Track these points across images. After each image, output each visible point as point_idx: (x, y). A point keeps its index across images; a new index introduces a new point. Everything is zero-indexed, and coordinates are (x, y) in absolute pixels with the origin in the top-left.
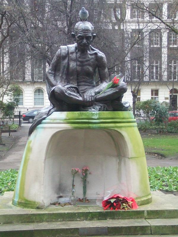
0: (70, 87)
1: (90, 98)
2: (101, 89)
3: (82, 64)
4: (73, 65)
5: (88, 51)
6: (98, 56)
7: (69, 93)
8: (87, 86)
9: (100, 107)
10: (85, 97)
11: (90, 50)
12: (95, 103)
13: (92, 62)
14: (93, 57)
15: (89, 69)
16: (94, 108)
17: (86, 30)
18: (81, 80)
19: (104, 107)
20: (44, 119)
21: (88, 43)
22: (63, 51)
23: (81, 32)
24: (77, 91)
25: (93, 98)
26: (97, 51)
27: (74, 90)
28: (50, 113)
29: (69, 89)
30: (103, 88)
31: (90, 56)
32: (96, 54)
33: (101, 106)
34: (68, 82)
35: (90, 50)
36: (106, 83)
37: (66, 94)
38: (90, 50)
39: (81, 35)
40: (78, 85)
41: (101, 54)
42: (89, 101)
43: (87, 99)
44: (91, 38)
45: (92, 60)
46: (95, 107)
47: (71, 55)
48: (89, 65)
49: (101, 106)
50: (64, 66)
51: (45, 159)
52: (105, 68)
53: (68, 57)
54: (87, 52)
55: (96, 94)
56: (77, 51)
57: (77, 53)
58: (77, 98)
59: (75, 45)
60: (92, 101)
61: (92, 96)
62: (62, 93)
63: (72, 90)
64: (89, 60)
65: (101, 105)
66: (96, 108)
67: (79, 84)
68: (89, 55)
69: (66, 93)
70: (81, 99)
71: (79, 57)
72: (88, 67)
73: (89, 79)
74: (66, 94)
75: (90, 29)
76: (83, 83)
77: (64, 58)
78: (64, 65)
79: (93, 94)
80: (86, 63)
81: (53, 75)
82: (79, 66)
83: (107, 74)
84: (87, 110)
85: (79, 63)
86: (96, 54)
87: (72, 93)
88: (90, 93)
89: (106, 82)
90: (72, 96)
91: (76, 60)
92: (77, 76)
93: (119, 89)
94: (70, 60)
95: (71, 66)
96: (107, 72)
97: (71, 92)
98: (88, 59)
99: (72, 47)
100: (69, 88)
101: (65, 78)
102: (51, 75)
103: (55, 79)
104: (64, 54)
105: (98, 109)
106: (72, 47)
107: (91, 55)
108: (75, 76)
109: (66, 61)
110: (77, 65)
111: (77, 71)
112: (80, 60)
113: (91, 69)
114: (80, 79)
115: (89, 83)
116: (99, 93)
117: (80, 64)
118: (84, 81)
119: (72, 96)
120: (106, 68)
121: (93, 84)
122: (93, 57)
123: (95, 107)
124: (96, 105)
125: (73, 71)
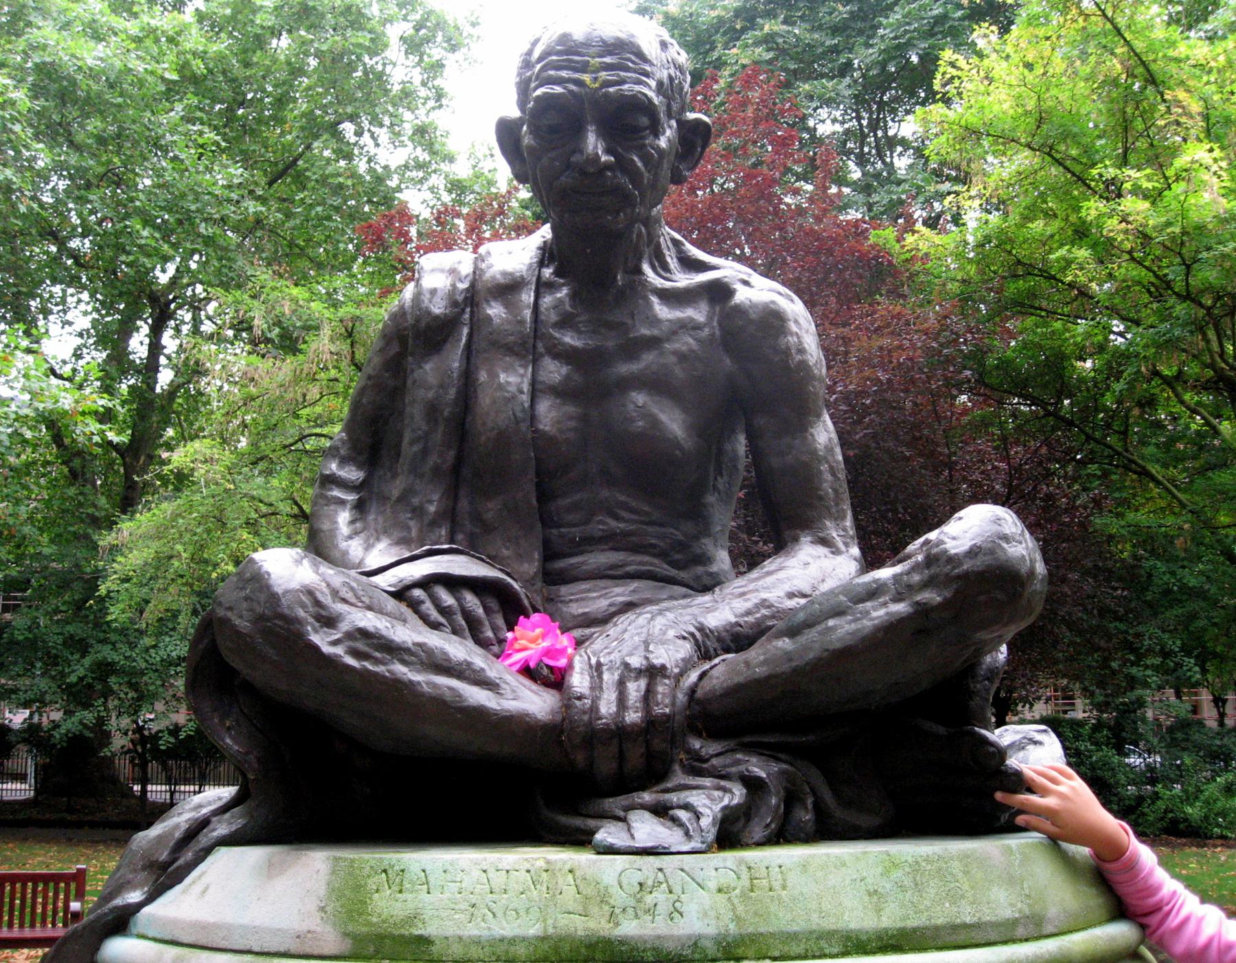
0: (427, 583)
1: (635, 689)
2: (764, 603)
5: (646, 268)
6: (740, 310)
7: (363, 633)
8: (635, 584)
9: (737, 794)
10: (579, 681)
11: (673, 263)
12: (689, 751)
13: (682, 357)
15: (655, 423)
16: (661, 811)
18: (576, 532)
19: (791, 799)
21: (622, 165)
23: (558, 68)
25: (662, 688)
27: (468, 616)
28: (189, 855)
29: (415, 606)
30: (791, 595)
31: (662, 311)
32: (719, 292)
33: (753, 785)
35: (666, 267)
36: (822, 550)
37: (316, 649)
38: (673, 263)
39: (558, 89)
42: (620, 733)
43: (594, 708)
44: (656, 131)
45: (687, 342)
46: (674, 798)
47: (495, 311)
48: (657, 385)
49: (753, 785)
50: (432, 410)
52: (802, 418)
53: (466, 331)
54: (640, 272)
55: (704, 654)
56: (547, 272)
57: (542, 287)
58: (476, 696)
60: (652, 724)
61: (653, 672)
63: (444, 611)
64: (653, 343)
65: (758, 768)
66: (683, 815)
67: (561, 564)
68: (654, 299)
69: (322, 640)
71: (566, 322)
72: (640, 398)
73: (656, 515)
74: (316, 639)
76: (599, 559)
78: (431, 395)
79: (671, 653)
80: (625, 369)
81: (351, 497)
82: (561, 392)
83: (833, 472)
84: (577, 822)
85: (554, 371)
87: (408, 633)
89: (825, 542)
90: (400, 669)
92: (544, 495)
93: (949, 580)
95: (485, 400)
96: (829, 449)
97: (435, 626)
98: (645, 331)
100: (417, 593)
101: (432, 509)
102: (337, 493)
104: (438, 308)
105: (705, 822)
107: (672, 297)
108: (527, 491)
109: (454, 359)
110: (536, 390)
111: (541, 442)
112: (569, 339)
114: (570, 518)
115: (662, 555)
117: (567, 378)
118: (611, 541)
119: (400, 669)
120: (819, 416)
121: (700, 570)
122: (697, 313)
123: (674, 798)
124: (697, 767)
125: (503, 438)
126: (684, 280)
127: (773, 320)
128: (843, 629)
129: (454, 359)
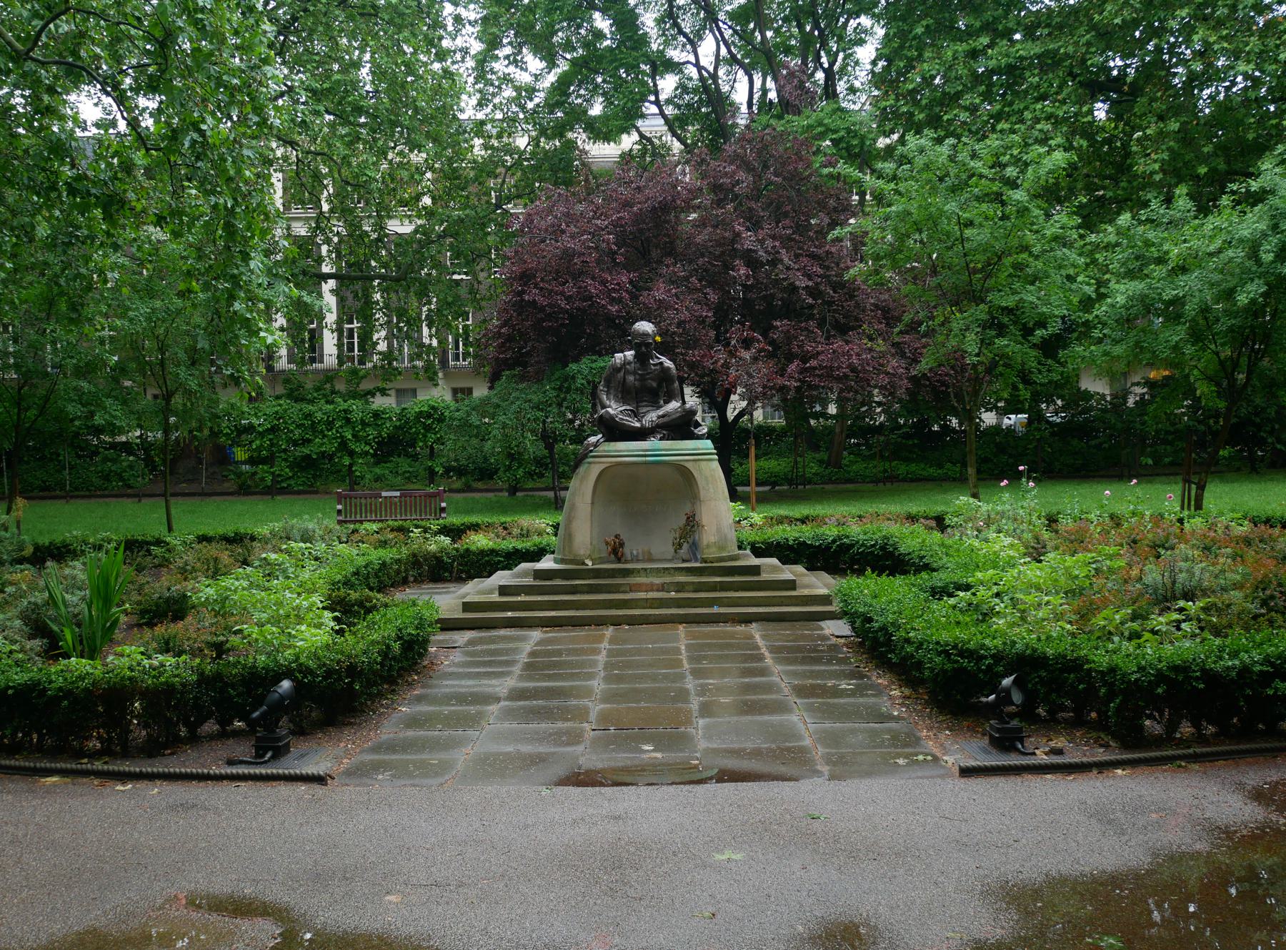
3: (642, 379)
4: (631, 378)
14: (658, 367)
17: (646, 335)
20: (591, 451)
22: (618, 361)
24: (635, 414)
26: (663, 359)
32: (661, 363)
34: (625, 403)
40: (637, 407)
41: (668, 363)
48: (652, 379)
51: (593, 503)
52: (673, 382)
59: (632, 352)
62: (612, 418)
70: (638, 425)
75: (650, 331)
77: (619, 370)
85: (638, 377)
86: (661, 363)
88: (652, 417)
91: (634, 373)
94: (627, 372)
99: (630, 354)
103: (608, 399)
106: (630, 354)
107: (654, 365)
109: (622, 373)
113: (655, 385)
116: (663, 416)
122: (658, 367)
126: (657, 361)
127: (669, 369)
128: (674, 416)
129: (622, 373)
